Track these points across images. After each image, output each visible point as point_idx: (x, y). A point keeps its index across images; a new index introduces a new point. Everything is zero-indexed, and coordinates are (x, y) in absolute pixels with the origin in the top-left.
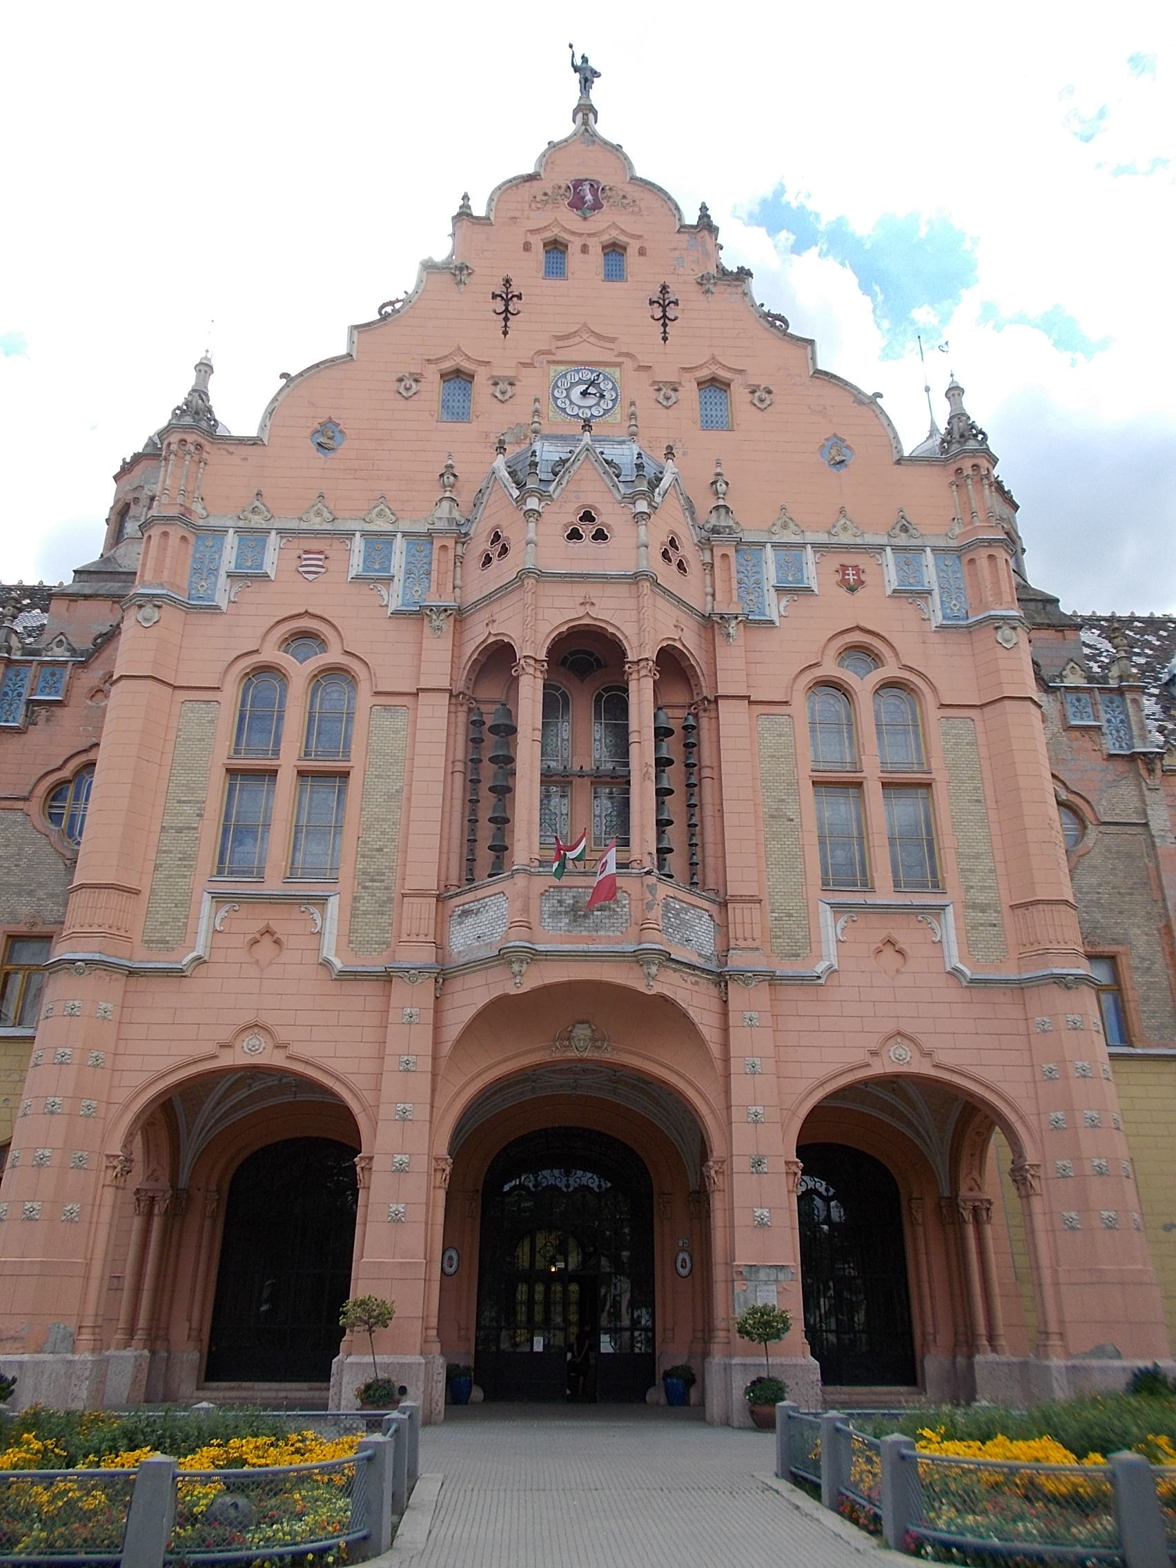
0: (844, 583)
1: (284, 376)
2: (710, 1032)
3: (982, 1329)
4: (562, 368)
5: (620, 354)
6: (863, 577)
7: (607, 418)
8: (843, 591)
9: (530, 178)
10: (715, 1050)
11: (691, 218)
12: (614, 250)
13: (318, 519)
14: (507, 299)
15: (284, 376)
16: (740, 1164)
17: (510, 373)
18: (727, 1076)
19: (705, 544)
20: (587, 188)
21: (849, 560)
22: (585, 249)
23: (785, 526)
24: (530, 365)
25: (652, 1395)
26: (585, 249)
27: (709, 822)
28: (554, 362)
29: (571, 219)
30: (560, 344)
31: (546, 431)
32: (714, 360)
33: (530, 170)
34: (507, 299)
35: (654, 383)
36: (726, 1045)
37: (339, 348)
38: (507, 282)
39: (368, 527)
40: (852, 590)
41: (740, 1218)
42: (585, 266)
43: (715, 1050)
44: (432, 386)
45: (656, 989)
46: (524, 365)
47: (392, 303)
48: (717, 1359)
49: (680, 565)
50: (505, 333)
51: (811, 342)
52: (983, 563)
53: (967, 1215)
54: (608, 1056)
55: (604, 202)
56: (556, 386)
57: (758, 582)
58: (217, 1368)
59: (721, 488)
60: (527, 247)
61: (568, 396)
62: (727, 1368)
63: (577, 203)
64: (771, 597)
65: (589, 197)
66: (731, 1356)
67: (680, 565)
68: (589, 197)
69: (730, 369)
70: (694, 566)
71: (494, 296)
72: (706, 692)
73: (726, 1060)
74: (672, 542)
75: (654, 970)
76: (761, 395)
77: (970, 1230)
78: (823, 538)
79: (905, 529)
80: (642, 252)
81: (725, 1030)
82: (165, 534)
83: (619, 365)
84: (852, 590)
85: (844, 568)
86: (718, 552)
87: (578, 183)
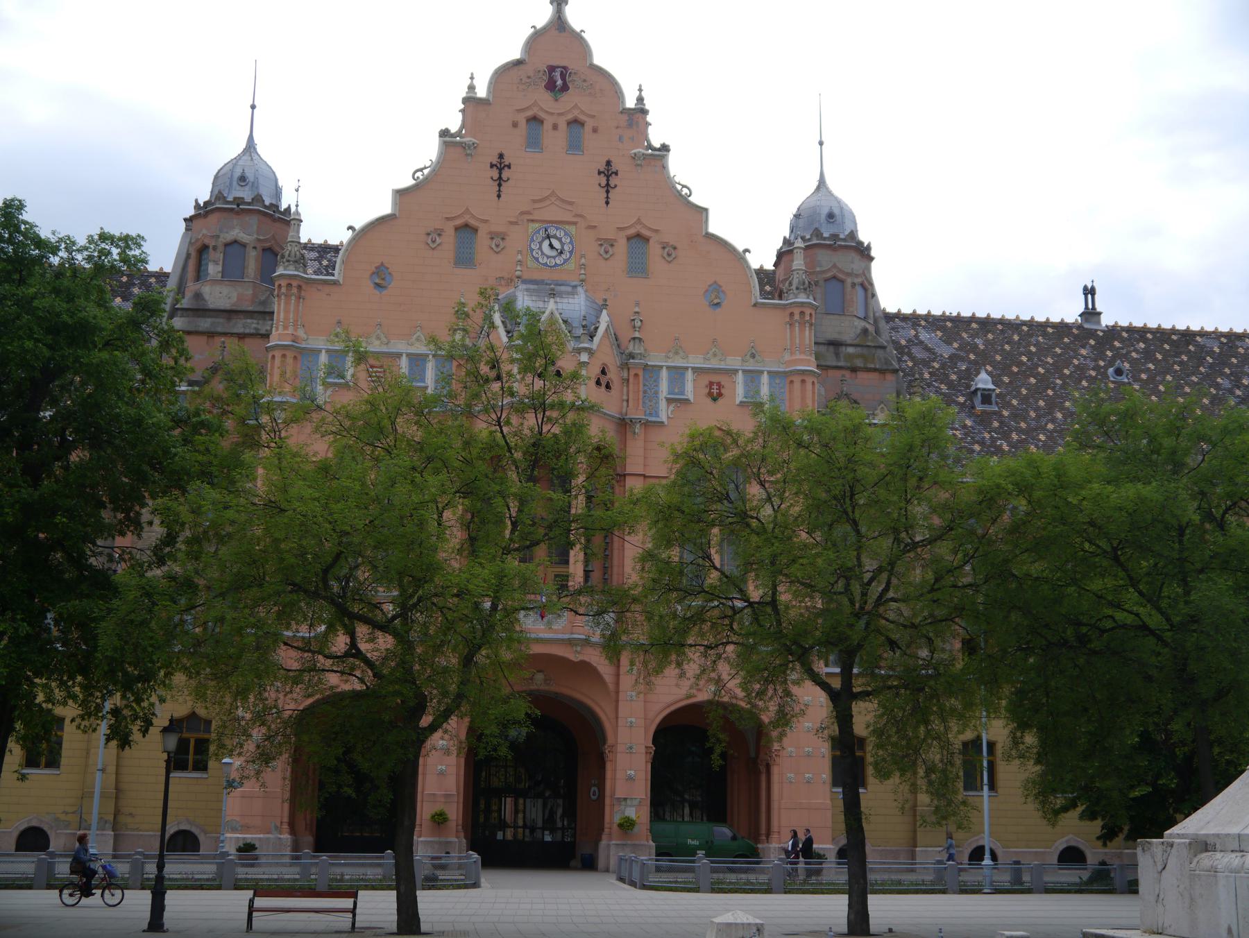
0: (710, 394)
1: (350, 228)
2: (608, 678)
3: (763, 830)
4: (537, 225)
5: (577, 216)
6: (723, 391)
7: (565, 267)
8: (709, 400)
9: (518, 63)
10: (611, 687)
11: (630, 103)
12: (576, 123)
13: (377, 342)
14: (501, 165)
15: (350, 228)
16: (620, 748)
17: (501, 229)
18: (617, 701)
19: (625, 366)
20: (557, 74)
21: (715, 379)
22: (555, 127)
23: (677, 353)
24: (516, 223)
25: (573, 863)
26: (555, 127)
27: (616, 553)
28: (533, 221)
29: (544, 99)
30: (537, 205)
31: (525, 277)
32: (639, 221)
33: (516, 54)
34: (501, 165)
35: (599, 239)
36: (617, 684)
37: (386, 208)
38: (501, 156)
39: (412, 350)
40: (715, 400)
41: (619, 775)
42: (555, 140)
43: (611, 687)
44: (449, 238)
45: (580, 658)
46: (511, 223)
47: (421, 170)
48: (603, 843)
49: (608, 387)
50: (499, 196)
51: (706, 210)
52: (797, 385)
53: (763, 769)
54: (554, 688)
55: (570, 85)
56: (532, 240)
57: (656, 393)
58: (320, 847)
59: (638, 324)
60: (515, 125)
61: (540, 248)
62: (609, 846)
63: (551, 86)
64: (663, 405)
65: (559, 82)
66: (610, 839)
67: (608, 387)
68: (559, 82)
69: (650, 229)
70: (616, 385)
71: (492, 166)
72: (619, 470)
73: (617, 692)
74: (603, 372)
75: (579, 649)
76: (670, 251)
77: (763, 778)
78: (700, 363)
79: (753, 356)
80: (595, 130)
81: (618, 675)
82: (284, 356)
83: (575, 223)
84: (715, 400)
85: (711, 384)
86: (632, 372)
87: (552, 69)
